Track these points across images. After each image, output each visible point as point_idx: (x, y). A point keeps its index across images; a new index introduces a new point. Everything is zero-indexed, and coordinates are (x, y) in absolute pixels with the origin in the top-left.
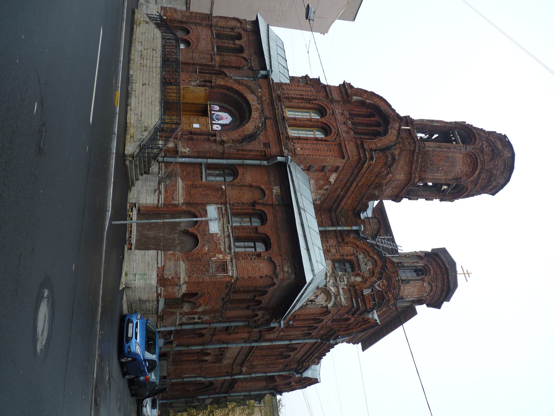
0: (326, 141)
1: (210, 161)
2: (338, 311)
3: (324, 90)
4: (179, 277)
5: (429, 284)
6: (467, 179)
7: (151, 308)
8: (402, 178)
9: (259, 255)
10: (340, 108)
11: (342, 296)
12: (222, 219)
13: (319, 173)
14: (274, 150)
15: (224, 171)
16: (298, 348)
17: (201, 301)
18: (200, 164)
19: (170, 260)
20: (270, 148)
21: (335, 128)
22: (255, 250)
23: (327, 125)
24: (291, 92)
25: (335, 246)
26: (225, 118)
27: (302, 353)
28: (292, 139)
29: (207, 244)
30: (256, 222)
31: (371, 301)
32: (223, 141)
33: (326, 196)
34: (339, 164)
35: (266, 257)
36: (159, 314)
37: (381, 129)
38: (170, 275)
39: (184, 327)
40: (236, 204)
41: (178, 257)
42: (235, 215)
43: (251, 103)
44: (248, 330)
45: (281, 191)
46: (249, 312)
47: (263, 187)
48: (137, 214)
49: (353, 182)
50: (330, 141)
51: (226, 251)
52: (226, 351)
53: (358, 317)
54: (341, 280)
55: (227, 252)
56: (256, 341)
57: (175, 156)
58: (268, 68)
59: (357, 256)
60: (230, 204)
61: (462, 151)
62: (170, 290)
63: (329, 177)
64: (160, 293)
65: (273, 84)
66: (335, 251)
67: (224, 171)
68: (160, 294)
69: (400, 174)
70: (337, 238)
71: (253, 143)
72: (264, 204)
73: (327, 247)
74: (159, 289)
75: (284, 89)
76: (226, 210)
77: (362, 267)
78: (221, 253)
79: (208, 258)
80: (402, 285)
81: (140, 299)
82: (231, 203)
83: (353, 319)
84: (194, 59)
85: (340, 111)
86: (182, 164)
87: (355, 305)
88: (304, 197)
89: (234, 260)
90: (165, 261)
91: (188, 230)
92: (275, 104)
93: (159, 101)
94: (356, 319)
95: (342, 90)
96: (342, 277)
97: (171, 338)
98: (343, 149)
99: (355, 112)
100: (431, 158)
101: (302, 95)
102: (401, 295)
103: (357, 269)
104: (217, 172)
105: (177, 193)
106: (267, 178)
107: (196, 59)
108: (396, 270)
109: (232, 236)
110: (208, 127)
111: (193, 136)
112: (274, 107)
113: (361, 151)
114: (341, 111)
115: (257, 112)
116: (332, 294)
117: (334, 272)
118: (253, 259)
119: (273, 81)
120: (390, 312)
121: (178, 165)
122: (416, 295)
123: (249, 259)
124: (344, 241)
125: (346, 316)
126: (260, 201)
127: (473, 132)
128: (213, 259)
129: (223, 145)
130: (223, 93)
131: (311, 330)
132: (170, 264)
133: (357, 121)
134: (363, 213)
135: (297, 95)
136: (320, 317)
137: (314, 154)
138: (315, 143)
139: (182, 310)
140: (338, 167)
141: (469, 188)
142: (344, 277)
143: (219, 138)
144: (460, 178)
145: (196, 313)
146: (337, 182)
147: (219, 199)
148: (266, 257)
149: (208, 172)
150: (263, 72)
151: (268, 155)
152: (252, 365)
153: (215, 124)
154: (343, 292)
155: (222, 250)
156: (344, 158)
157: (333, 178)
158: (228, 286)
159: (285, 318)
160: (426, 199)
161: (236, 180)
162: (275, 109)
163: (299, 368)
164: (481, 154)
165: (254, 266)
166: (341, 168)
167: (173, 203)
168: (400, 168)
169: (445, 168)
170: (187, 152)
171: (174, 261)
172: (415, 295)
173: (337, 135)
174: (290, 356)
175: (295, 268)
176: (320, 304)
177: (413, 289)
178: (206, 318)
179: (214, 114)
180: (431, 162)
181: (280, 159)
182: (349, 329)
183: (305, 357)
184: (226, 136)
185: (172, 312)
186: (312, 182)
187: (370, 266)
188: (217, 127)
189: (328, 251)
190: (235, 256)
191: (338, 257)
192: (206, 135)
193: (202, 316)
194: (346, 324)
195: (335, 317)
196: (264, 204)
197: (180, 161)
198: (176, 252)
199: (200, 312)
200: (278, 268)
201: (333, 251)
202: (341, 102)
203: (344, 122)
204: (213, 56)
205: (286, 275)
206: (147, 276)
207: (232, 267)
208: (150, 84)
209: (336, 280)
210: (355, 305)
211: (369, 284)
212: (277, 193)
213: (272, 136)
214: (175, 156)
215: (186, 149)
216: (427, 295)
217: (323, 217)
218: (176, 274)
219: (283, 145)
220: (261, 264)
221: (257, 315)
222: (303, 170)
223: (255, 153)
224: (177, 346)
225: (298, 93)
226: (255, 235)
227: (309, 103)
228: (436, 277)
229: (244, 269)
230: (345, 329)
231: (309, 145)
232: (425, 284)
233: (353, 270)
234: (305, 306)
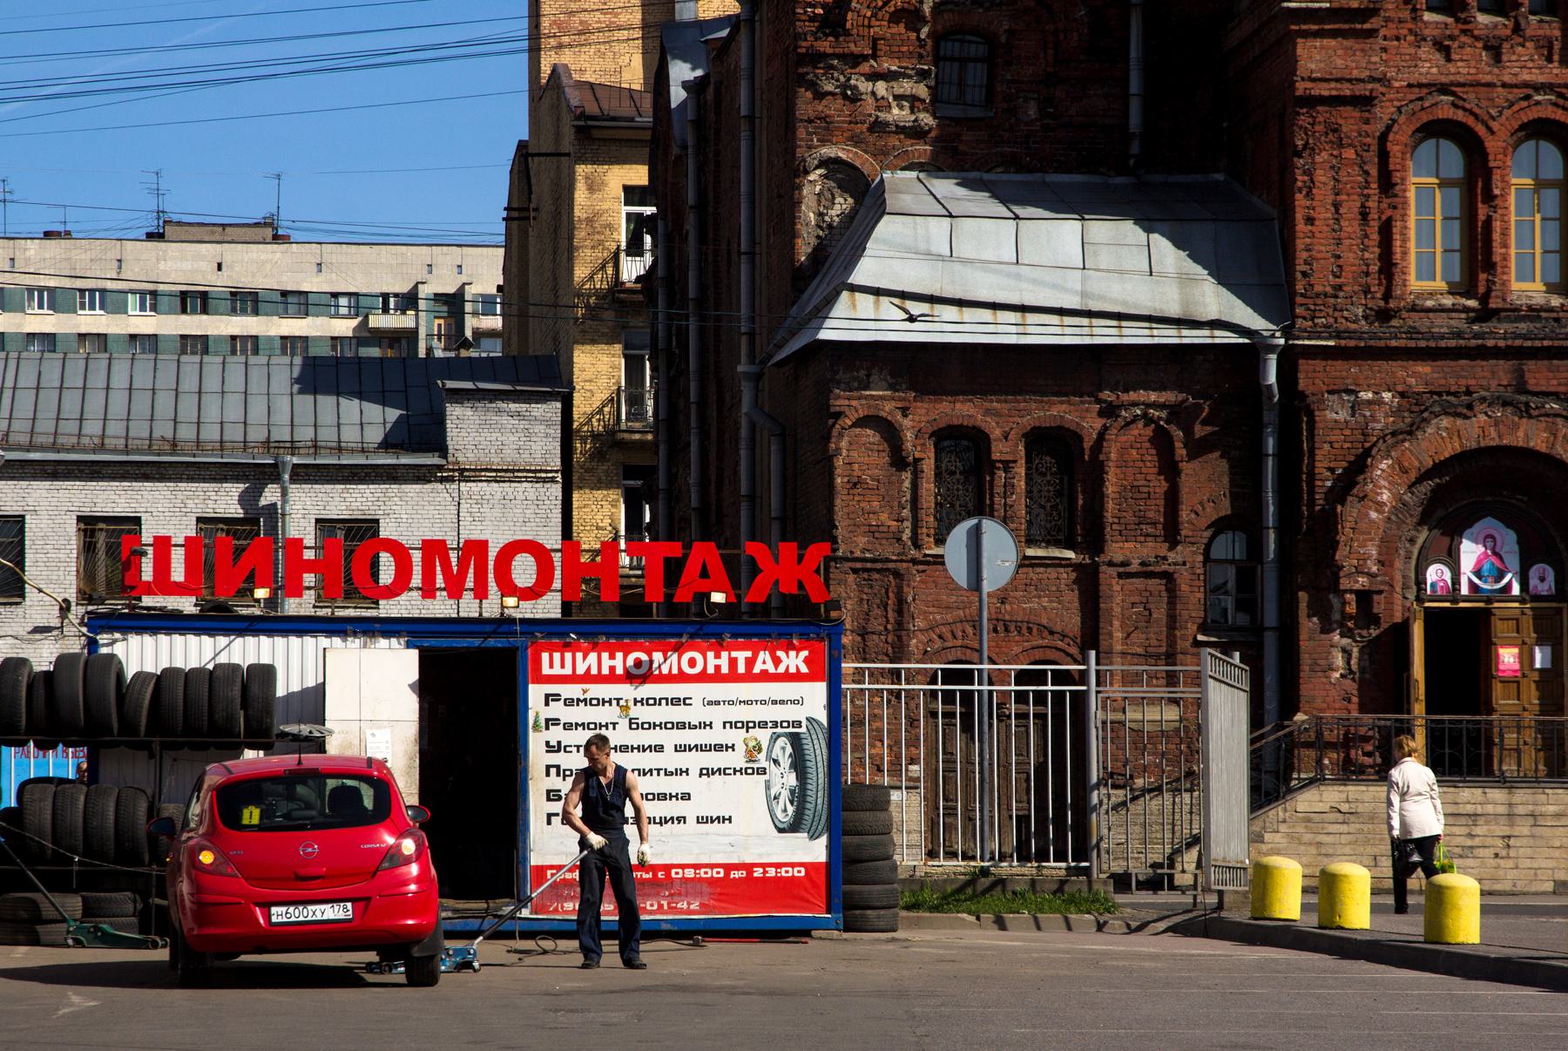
24: (1349, 257)
135: (1366, 236)
179: (1471, 584)
188: (1542, 579)
204: (1128, 569)
225: (1351, 226)
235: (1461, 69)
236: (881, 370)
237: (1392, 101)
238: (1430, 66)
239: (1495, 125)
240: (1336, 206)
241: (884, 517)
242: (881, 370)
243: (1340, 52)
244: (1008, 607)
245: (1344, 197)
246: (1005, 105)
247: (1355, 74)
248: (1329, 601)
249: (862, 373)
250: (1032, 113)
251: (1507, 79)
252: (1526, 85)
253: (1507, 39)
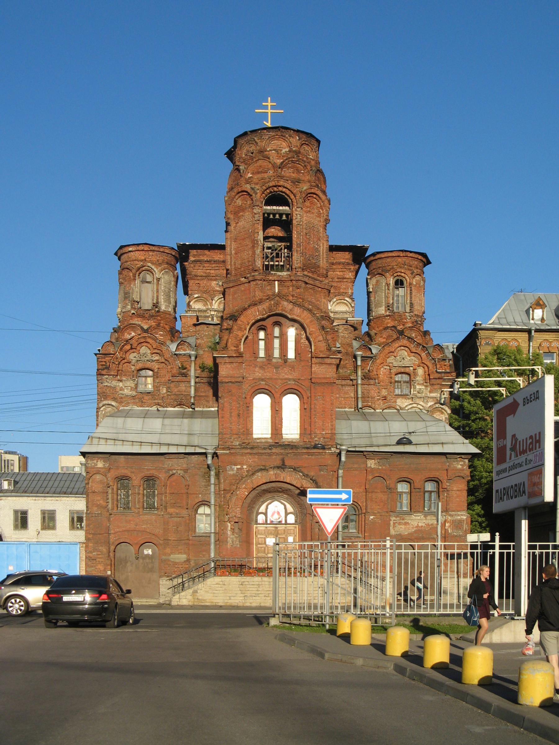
137: (330, 416)
153: (286, 521)
165: (455, 495)
205: (465, 467)
212: (375, 464)
235: (268, 375)
236: (101, 460)
237: (247, 383)
238: (259, 373)
239: (277, 390)
240: (231, 413)
241: (101, 502)
242: (101, 460)
243: (231, 369)
244: (138, 527)
245: (233, 411)
246: (156, 389)
247: (236, 375)
248: (227, 525)
249: (95, 461)
250: (165, 391)
251: (281, 377)
252: (286, 379)
253: (282, 366)
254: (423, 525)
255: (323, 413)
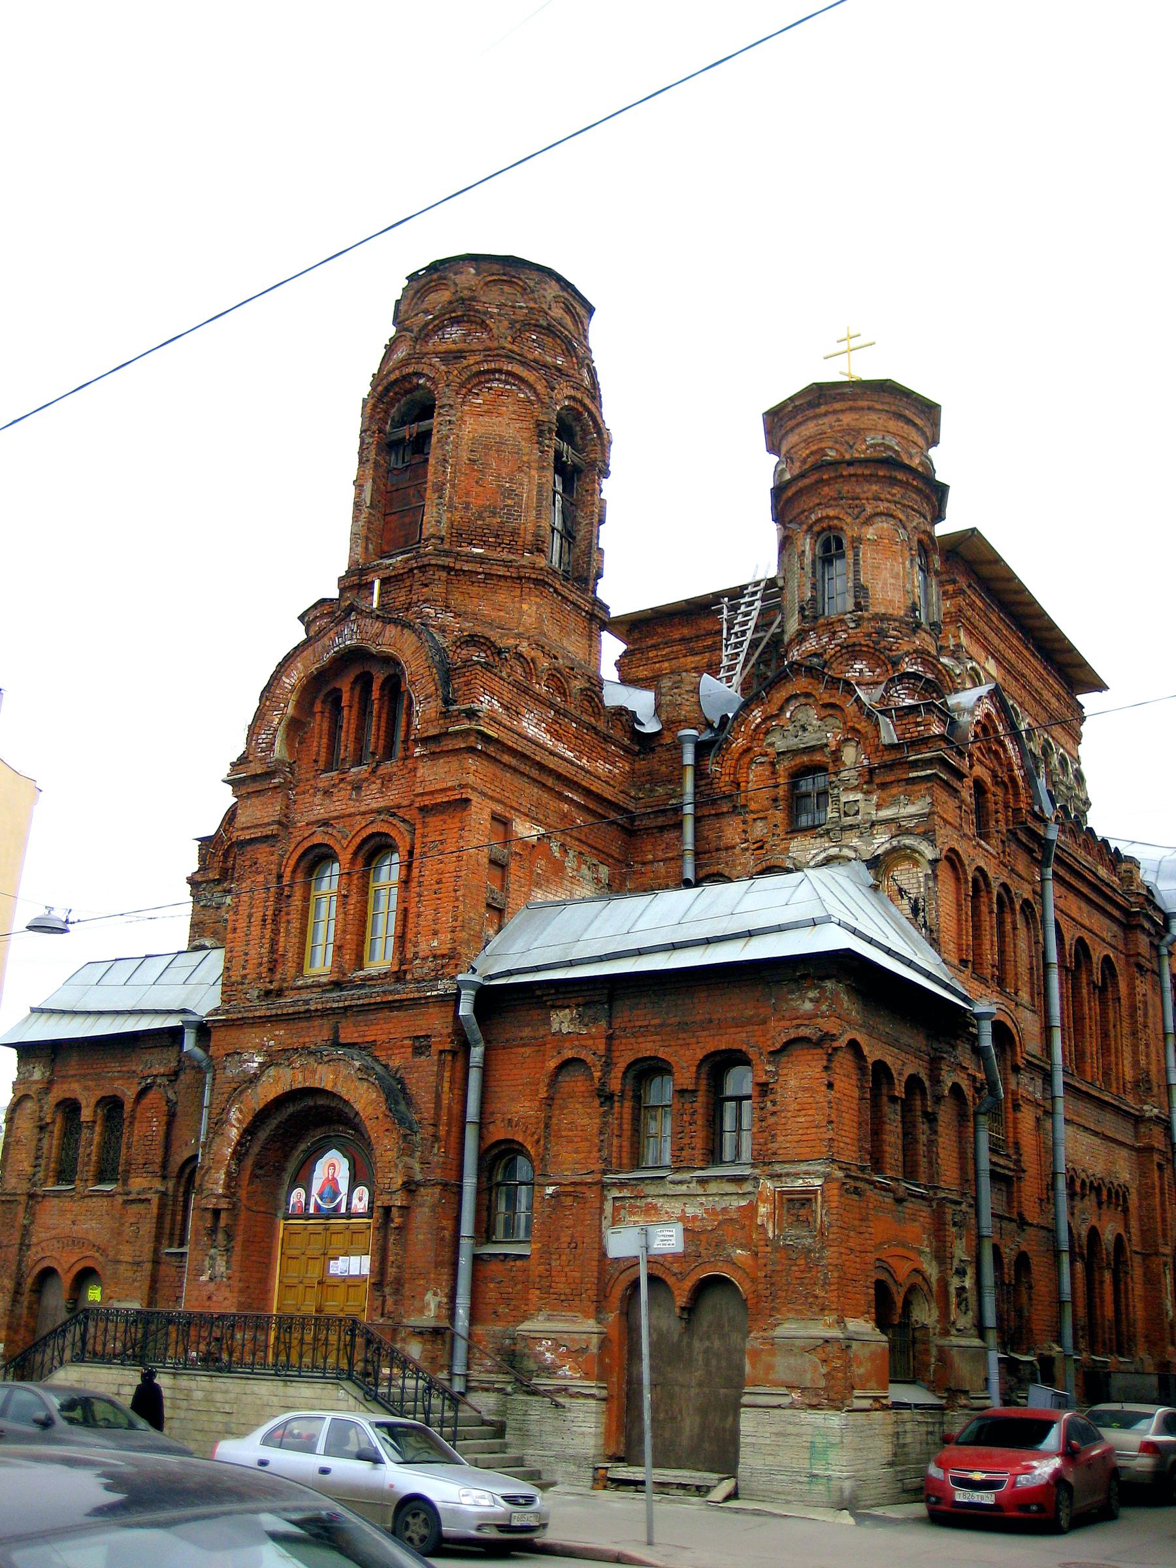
0: (411, 853)
1: (467, 1228)
2: (950, 824)
3: (249, 848)
4: (821, 1341)
5: (868, 521)
6: (543, 403)
7: (923, 1429)
8: (534, 608)
9: (764, 1089)
10: (307, 798)
11: (902, 810)
12: (649, 1200)
13: (512, 878)
14: (436, 1023)
15: (499, 1185)
16: (1078, 935)
17: (903, 1270)
18: (477, 1259)
19: (770, 1368)
20: (429, 1036)
21: (372, 822)
22: (748, 1098)
23: (360, 847)
25: (745, 822)
26: (331, 1171)
27: (1095, 921)
28: (402, 963)
29: (724, 1249)
30: (661, 1091)
31: (919, 720)
32: (404, 1183)
33: (585, 849)
34: (486, 815)
35: (769, 1068)
36: (943, 1402)
37: (379, 677)
38: (815, 1368)
39: (990, 1320)
40: (605, 1153)
41: (762, 1344)
42: (636, 1162)
43: (287, 1088)
44: (1011, 1110)
45: (568, 1007)
46: (946, 1114)
47: (552, 1064)
48: (629, 1465)
49: (542, 767)
50: (412, 840)
51: (749, 1193)
52: (1083, 1175)
53: (971, 755)
54: (852, 813)
55: (751, 1189)
56: (1048, 1078)
57: (448, 1340)
58: (173, 1022)
59: (779, 754)
60: (604, 1172)
61: (453, 419)
62: (862, 1371)
63: (526, 845)
64: (871, 1401)
65: (227, 1012)
66: (760, 824)
67: (499, 1185)
68: (876, 1399)
69: (521, 612)
70: (718, 815)
71: (412, 1090)
72: (608, 1065)
73: (747, 849)
74: (858, 1404)
75: (244, 976)
76: (622, 1185)
77: (813, 739)
78: (752, 1209)
79: (769, 1249)
80: (872, 610)
81: (891, 1464)
82: (603, 1166)
83: (978, 770)
84: (137, 1259)
85: (318, 799)
86: (473, 1318)
87: (929, 772)
88: (586, 930)
89: (778, 1168)
90: (776, 1384)
91: (683, 1309)
92: (291, 1010)
93: (281, 1383)
94: (978, 759)
95: (250, 790)
96: (842, 806)
97: (1030, 1362)
98: (439, 800)
99: (323, 751)
100: (473, 514)
101: (264, 920)
102: (902, 613)
103: (818, 757)
104: (502, 1207)
105: (565, 1336)
106: (523, 1050)
107: (138, 1253)
108: (823, 625)
109: (702, 1169)
110: (356, 1227)
111: (390, 1278)
112: (300, 1013)
113: (450, 744)
114: (319, 796)
115: (314, 1072)
116: (895, 843)
117: (828, 832)
118: (775, 1109)
119: (216, 1011)
120: (969, 614)
121: (479, 1329)
122: (903, 563)
123: (772, 1120)
124: (731, 796)
125: (967, 794)
126: (597, 1074)
127: (396, 381)
128: (771, 1235)
129: (418, 1184)
130: (254, 1176)
131: (1012, 902)
132: (783, 1366)
133: (351, 746)
134: (643, 724)
136: (966, 881)
137: (452, 894)
138: (417, 889)
139: (934, 1328)
140: (495, 817)
141: (572, 392)
142: (843, 799)
143: (395, 1197)
144: (539, 424)
145: (944, 1284)
146: (541, 817)
147: (587, 1205)
148: (769, 1068)
149: (499, 1234)
150: (189, 1042)
151: (452, 1042)
152: (1137, 1084)
153: (349, 1203)
154: (888, 807)
155: (743, 1203)
156: (468, 800)
157: (526, 830)
158: (856, 1188)
159: (965, 999)
160: (602, 521)
161: (529, 1148)
162: (308, 1011)
163: (1147, 925)
164: (465, 358)
165: (794, 1106)
166: (499, 808)
167: (595, 1351)
168: (501, 613)
169: (504, 471)
170: (438, 1299)
171: (774, 1355)
172: (904, 568)
173: (393, 815)
174: (1107, 958)
175: (804, 977)
176: (926, 884)
177: (884, 572)
178: (960, 1251)
179: (317, 1207)
180: (485, 514)
181: (465, 1009)
182: (1013, 779)
183: (1109, 908)
184: (391, 1175)
185: (939, 1360)
186: (539, 896)
187: (811, 715)
188: (360, 1199)
189: (761, 848)
190: (765, 1164)
191: (779, 816)
192: (385, 1238)
193: (956, 1263)
194: (993, 789)
195: (970, 830)
196: (608, 1065)
197: (466, 1323)
198: (748, 1346)
199: (940, 1272)
200: (804, 1032)
201: (759, 830)
202: (288, 795)
203: (353, 789)
204: (130, 1198)
205: (824, 1008)
206: (818, 1439)
207: (797, 1175)
208: (227, 1409)
209: (852, 827)
210: (929, 772)
211: (863, 724)
212: (572, 1020)
213: (391, 1025)
214: (448, 1340)
215: (429, 1304)
216: (905, 528)
217: (650, 857)
218: (812, 1350)
219: (422, 994)
220: (792, 1083)
221: (956, 1089)
222: (500, 929)
223: (446, 1085)
224: (1059, 1340)
225: (256, 931)
226: (701, 1099)
227: (289, 897)
228: (847, 498)
229: (804, 1137)
230: (1011, 791)
231: (422, 909)
232: (870, 533)
233: (821, 768)
234: (931, 931)
253: (367, 779)
254: (699, 1212)
255: (437, 886)
